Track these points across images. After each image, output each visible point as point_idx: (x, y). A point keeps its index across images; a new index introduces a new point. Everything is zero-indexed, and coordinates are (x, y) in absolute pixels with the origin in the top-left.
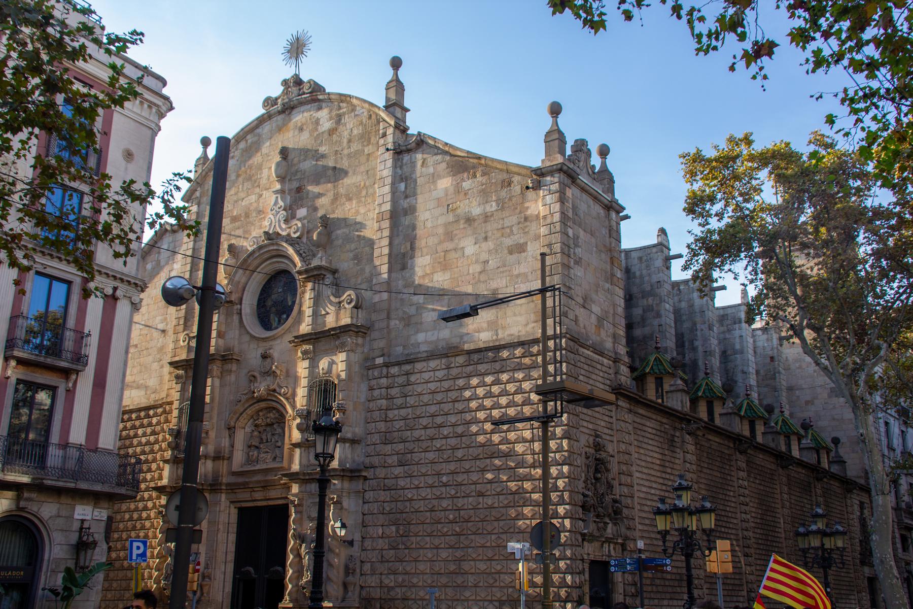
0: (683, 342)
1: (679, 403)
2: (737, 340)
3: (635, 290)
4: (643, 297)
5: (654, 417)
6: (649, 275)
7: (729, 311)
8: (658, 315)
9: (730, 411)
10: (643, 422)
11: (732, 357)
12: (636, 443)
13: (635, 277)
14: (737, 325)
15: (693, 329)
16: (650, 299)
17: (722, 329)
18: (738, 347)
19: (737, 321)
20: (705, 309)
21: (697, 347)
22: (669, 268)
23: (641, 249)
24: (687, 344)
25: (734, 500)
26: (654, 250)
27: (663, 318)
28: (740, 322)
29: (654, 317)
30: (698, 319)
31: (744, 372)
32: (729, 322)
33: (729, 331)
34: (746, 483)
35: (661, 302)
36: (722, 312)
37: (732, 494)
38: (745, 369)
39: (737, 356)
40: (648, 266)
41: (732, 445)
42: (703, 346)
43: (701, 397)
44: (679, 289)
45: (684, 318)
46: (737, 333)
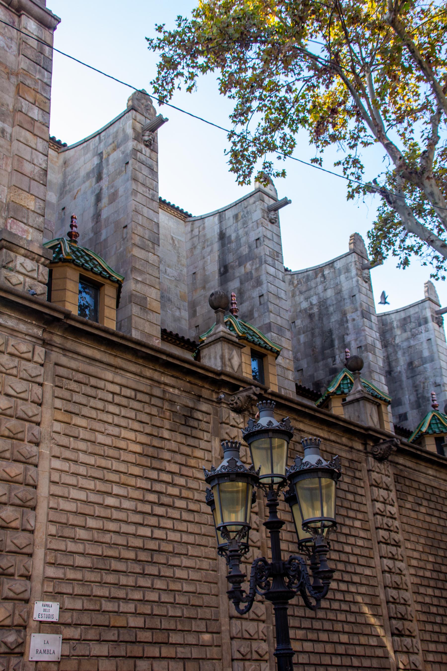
0: (332, 341)
1: (219, 360)
2: (425, 345)
3: (231, 258)
4: (240, 265)
5: (133, 368)
6: (247, 234)
7: (412, 311)
8: (259, 283)
9: (358, 396)
10: (92, 369)
11: (421, 368)
12: (58, 403)
13: (230, 242)
14: (423, 327)
15: (343, 322)
16: (248, 266)
17: (405, 335)
18: (426, 354)
19: (422, 321)
20: (356, 292)
21: (349, 343)
22: (275, 221)
23: (236, 204)
24: (336, 343)
25: (362, 534)
26: (252, 200)
27: (265, 286)
28: (426, 322)
29: (254, 287)
30: (348, 307)
31: (437, 385)
32: (413, 325)
33: (414, 336)
34: (394, 510)
35: (261, 265)
36: (403, 315)
37: (358, 524)
38: (438, 380)
39: (428, 365)
40: (245, 224)
41: (361, 447)
42: (356, 340)
43: (334, 393)
44: (323, 276)
45: (331, 309)
46: (423, 337)
